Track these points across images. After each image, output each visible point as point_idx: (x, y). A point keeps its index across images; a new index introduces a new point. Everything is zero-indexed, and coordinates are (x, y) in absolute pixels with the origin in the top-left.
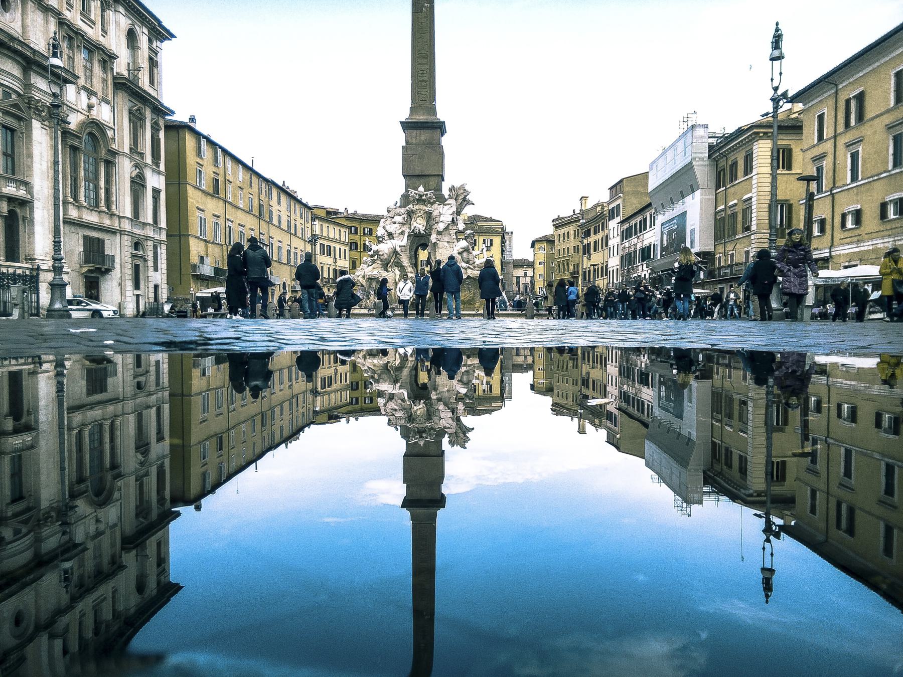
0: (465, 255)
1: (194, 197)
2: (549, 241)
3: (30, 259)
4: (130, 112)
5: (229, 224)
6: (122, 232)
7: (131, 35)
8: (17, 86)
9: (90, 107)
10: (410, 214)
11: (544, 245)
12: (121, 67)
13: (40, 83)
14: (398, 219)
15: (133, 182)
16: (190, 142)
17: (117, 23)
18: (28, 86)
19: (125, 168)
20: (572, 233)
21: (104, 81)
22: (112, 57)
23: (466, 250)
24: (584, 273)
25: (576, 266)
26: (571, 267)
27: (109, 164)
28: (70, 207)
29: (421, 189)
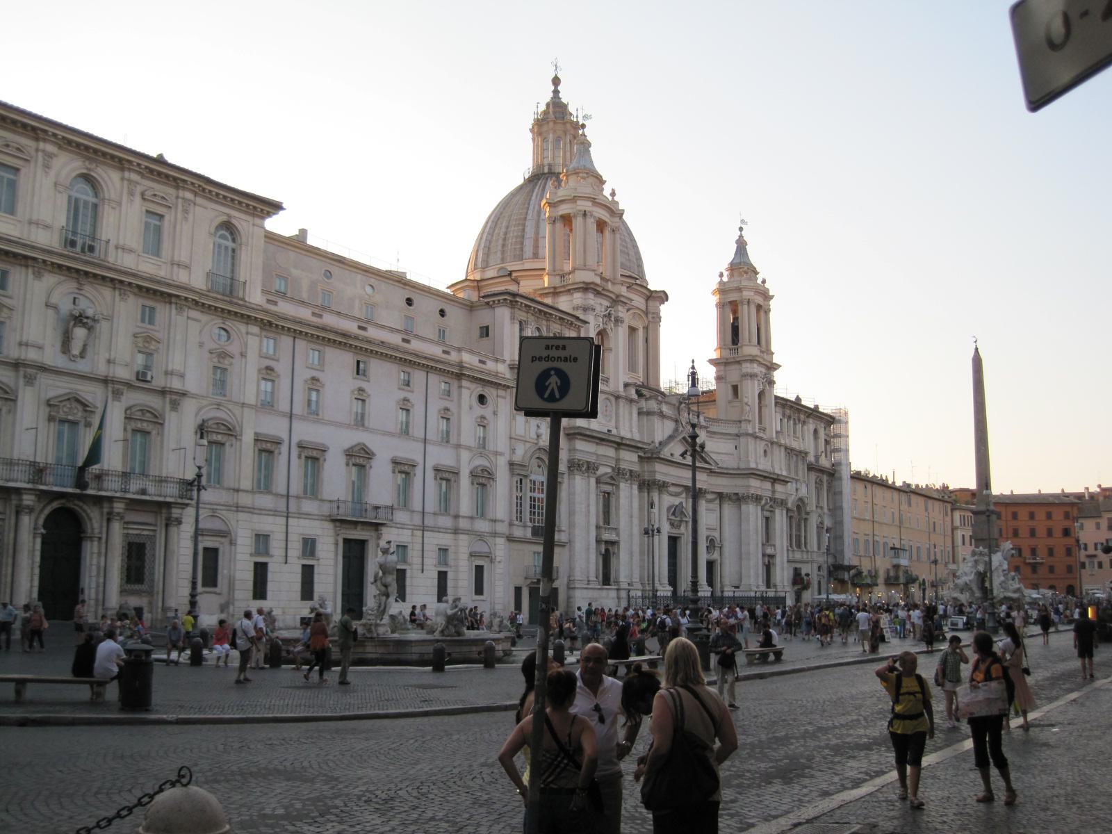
0: (1003, 584)
3: (775, 586)
4: (816, 483)
5: (876, 538)
6: (812, 562)
7: (816, 431)
8: (769, 494)
9: (797, 490)
10: (976, 562)
12: (811, 458)
13: (778, 487)
14: (970, 564)
15: (818, 527)
17: (808, 430)
18: (774, 492)
19: (814, 521)
21: (804, 469)
22: (806, 453)
23: (1003, 582)
27: (806, 520)
28: (790, 552)
29: (981, 548)
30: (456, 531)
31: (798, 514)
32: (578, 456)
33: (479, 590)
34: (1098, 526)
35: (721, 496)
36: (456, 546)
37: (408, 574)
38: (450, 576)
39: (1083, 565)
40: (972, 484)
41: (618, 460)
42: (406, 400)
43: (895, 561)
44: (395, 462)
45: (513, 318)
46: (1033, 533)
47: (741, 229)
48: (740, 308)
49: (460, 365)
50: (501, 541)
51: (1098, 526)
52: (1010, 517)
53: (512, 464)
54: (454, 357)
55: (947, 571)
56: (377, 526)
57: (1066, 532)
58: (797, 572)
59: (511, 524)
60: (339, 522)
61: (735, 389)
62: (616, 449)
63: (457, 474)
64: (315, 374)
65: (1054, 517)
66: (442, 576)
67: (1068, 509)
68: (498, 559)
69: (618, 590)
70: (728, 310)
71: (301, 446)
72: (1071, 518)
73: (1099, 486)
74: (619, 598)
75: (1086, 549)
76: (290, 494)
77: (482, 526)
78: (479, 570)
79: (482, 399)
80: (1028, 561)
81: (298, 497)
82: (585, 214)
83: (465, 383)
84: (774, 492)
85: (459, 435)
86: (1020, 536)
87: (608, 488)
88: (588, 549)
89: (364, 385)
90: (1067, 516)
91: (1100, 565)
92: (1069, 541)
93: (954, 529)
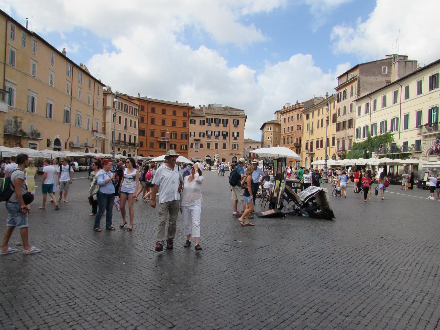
2: (277, 125)
11: (272, 127)
24: (307, 144)
25: (299, 140)
26: (295, 141)
39: (192, 146)
46: (163, 123)
52: (150, 111)
55: (93, 138)
57: (185, 125)
65: (178, 114)
67: (186, 111)
72: (187, 116)
73: (200, 106)
75: (194, 136)
80: (159, 140)
86: (156, 123)
90: (185, 115)
91: (202, 146)
92: (184, 130)
93: (105, 109)
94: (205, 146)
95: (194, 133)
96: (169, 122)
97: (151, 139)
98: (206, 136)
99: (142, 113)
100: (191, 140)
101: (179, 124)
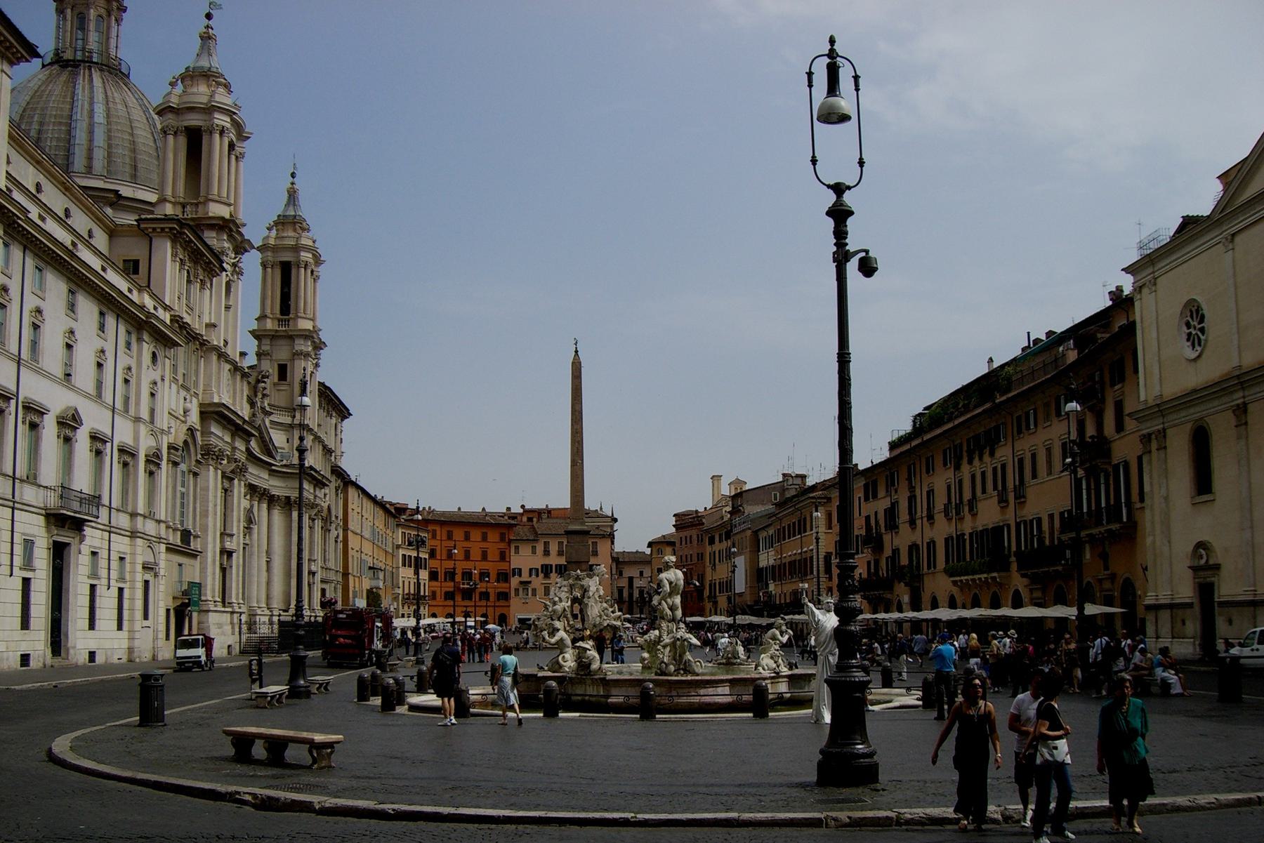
1: (353, 542)
16: (352, 492)
18: (315, 496)
19: (334, 533)
20: (695, 537)
30: (133, 534)
31: (327, 521)
32: (213, 440)
33: (146, 617)
34: (534, 552)
35: (272, 500)
36: (133, 554)
37: (98, 591)
38: (126, 594)
40: (561, 500)
41: (234, 449)
42: (103, 351)
43: (374, 583)
44: (95, 437)
45: (174, 255)
47: (293, 175)
48: (294, 271)
49: (142, 308)
50: (163, 547)
51: (534, 552)
53: (169, 448)
54: (135, 297)
56: (77, 525)
57: (503, 557)
58: (323, 591)
59: (168, 527)
60: (56, 519)
61: (283, 371)
62: (233, 436)
63: (133, 456)
64: (38, 302)
66: (121, 590)
68: (162, 572)
69: (232, 613)
70: (278, 272)
71: (29, 408)
73: (523, 507)
74: (232, 623)
75: (520, 575)
76: (18, 475)
77: (150, 527)
78: (147, 582)
79: (154, 356)
81: (22, 481)
82: (222, 133)
83: (146, 337)
84: (315, 496)
85: (138, 403)
87: (227, 485)
88: (214, 561)
89: (73, 324)
91: (534, 591)
92: (503, 566)
94: (540, 591)
95: (520, 570)
96: (476, 554)
97: (449, 586)
98: (541, 575)
99: (434, 542)
100: (515, 581)
101: (493, 554)
